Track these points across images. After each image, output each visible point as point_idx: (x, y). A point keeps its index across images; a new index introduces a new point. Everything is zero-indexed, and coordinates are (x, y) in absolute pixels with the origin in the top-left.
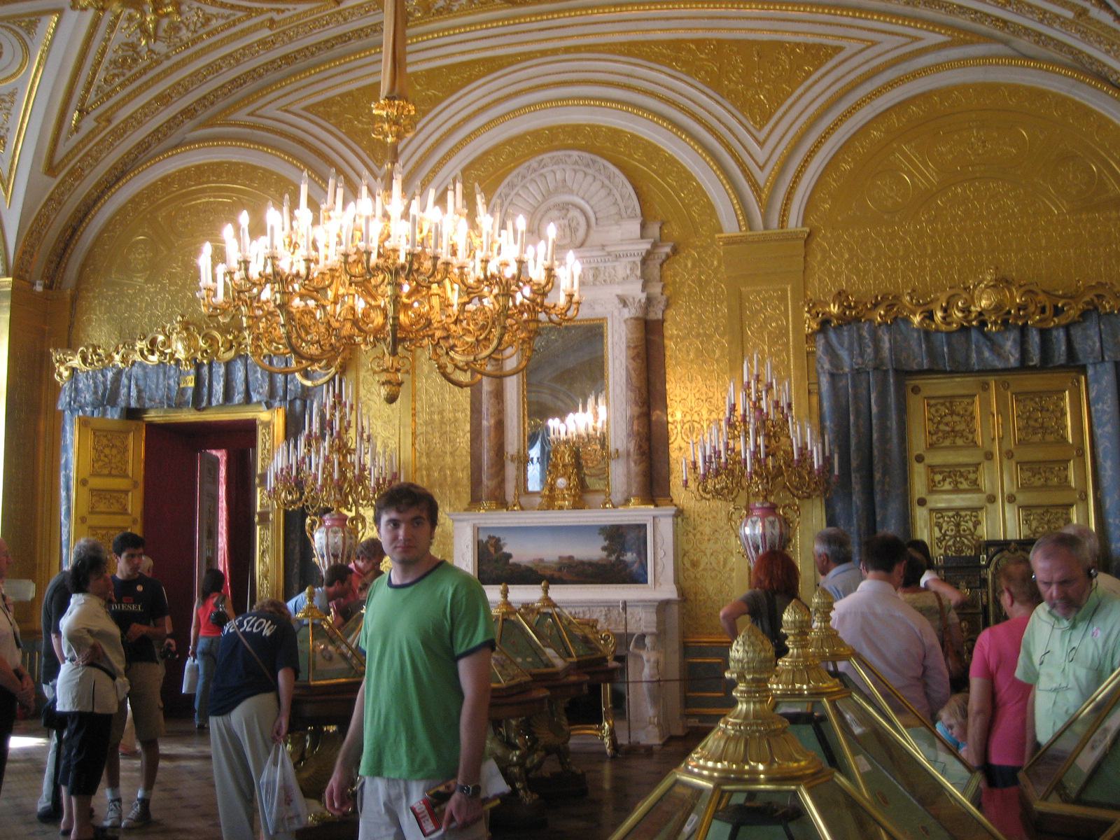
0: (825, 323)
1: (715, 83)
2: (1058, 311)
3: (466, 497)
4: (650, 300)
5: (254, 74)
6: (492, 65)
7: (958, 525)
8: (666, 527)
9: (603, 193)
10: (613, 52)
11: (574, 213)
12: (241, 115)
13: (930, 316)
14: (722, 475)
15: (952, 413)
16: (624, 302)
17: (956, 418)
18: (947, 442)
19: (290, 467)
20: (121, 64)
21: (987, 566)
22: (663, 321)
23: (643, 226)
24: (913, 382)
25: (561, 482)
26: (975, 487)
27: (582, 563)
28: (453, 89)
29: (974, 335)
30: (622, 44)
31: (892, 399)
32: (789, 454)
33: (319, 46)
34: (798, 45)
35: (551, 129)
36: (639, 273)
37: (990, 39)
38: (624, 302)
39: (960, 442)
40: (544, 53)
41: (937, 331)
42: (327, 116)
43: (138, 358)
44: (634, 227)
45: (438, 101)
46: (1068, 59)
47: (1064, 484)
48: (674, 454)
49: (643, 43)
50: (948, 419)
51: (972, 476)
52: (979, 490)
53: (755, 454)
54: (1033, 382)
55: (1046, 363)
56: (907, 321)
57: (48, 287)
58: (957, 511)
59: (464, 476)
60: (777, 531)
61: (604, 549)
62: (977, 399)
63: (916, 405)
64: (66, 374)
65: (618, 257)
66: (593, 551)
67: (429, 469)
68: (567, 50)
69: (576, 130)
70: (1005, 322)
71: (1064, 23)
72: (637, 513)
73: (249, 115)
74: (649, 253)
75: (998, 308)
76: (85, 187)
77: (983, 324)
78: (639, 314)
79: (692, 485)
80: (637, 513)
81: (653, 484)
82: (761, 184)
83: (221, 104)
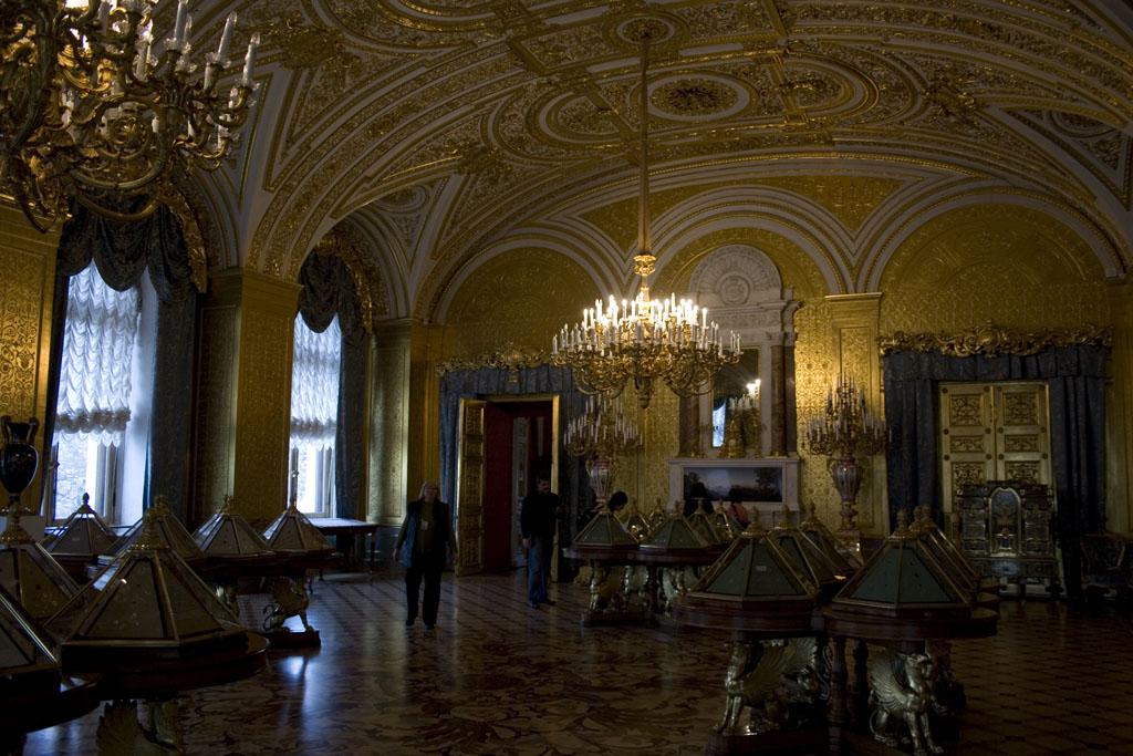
0: (888, 352)
2: (1030, 346)
3: (678, 450)
4: (786, 335)
5: (550, 195)
7: (968, 472)
8: (794, 468)
9: (759, 270)
11: (740, 282)
12: (541, 220)
13: (952, 346)
14: (822, 443)
15: (966, 404)
16: (770, 337)
17: (969, 408)
18: (963, 422)
19: (578, 432)
20: (477, 197)
22: (794, 347)
23: (782, 291)
24: (942, 386)
25: (732, 442)
26: (980, 449)
29: (978, 358)
31: (929, 397)
32: (861, 429)
33: (588, 180)
34: (877, 179)
36: (779, 319)
37: (997, 176)
38: (770, 337)
39: (970, 422)
41: (956, 356)
43: (484, 364)
44: (777, 292)
46: (1044, 190)
48: (799, 427)
49: (785, 178)
50: (964, 408)
51: (978, 443)
52: (982, 452)
53: (841, 430)
54: (1014, 387)
55: (1024, 377)
56: (938, 350)
57: (430, 322)
58: (968, 463)
59: (676, 437)
60: (855, 473)
61: (757, 481)
62: (982, 398)
63: (944, 398)
64: (442, 373)
65: (767, 310)
66: (751, 482)
67: (655, 432)
68: (738, 182)
69: (742, 232)
70: (997, 353)
71: (1035, 172)
72: (777, 460)
73: (548, 219)
74: (785, 307)
75: (993, 343)
76: (450, 265)
77: (984, 353)
78: (780, 343)
79: (807, 447)
80: (777, 460)
81: (786, 442)
82: (854, 264)
83: (530, 213)
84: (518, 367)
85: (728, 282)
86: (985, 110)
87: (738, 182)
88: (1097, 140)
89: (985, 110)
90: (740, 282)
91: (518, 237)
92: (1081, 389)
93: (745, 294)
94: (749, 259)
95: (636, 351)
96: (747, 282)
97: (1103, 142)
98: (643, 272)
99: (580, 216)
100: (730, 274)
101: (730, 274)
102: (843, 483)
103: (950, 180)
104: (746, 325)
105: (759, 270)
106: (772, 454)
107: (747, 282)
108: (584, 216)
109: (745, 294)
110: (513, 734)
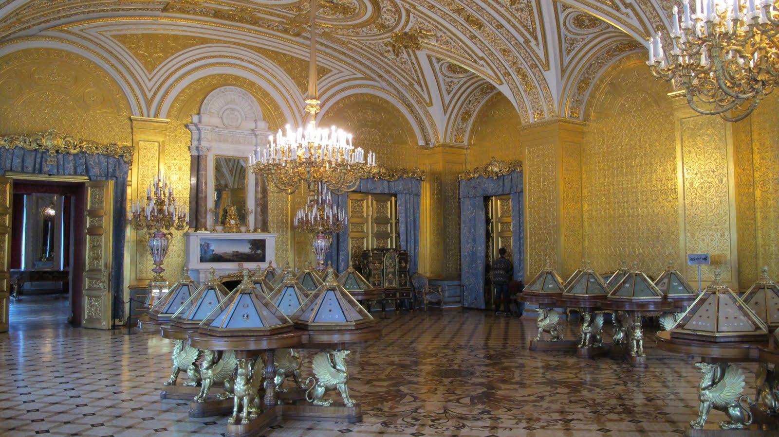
1: (289, 72)
6: (204, 41)
9: (249, 107)
10: (252, 49)
11: (236, 113)
21: (384, 257)
27: (241, 254)
28: (185, 47)
30: (257, 47)
35: (226, 75)
40: (225, 42)
42: (124, 43)
45: (177, 51)
47: (362, 231)
66: (246, 249)
68: (235, 43)
71: (403, 85)
77: (374, 177)
84: (57, 151)
85: (228, 112)
86: (417, 52)
87: (235, 43)
88: (450, 80)
89: (417, 52)
90: (236, 113)
91: (53, 38)
92: (412, 201)
93: (240, 121)
94: (243, 98)
95: (310, 163)
96: (240, 114)
97: (451, 82)
98: (313, 111)
99: (331, 71)
100: (228, 107)
101: (228, 107)
102: (322, 250)
103: (355, 76)
104: (240, 143)
105: (249, 107)
106: (255, 231)
107: (240, 114)
108: (114, 36)
109: (240, 121)
110: (460, 401)
